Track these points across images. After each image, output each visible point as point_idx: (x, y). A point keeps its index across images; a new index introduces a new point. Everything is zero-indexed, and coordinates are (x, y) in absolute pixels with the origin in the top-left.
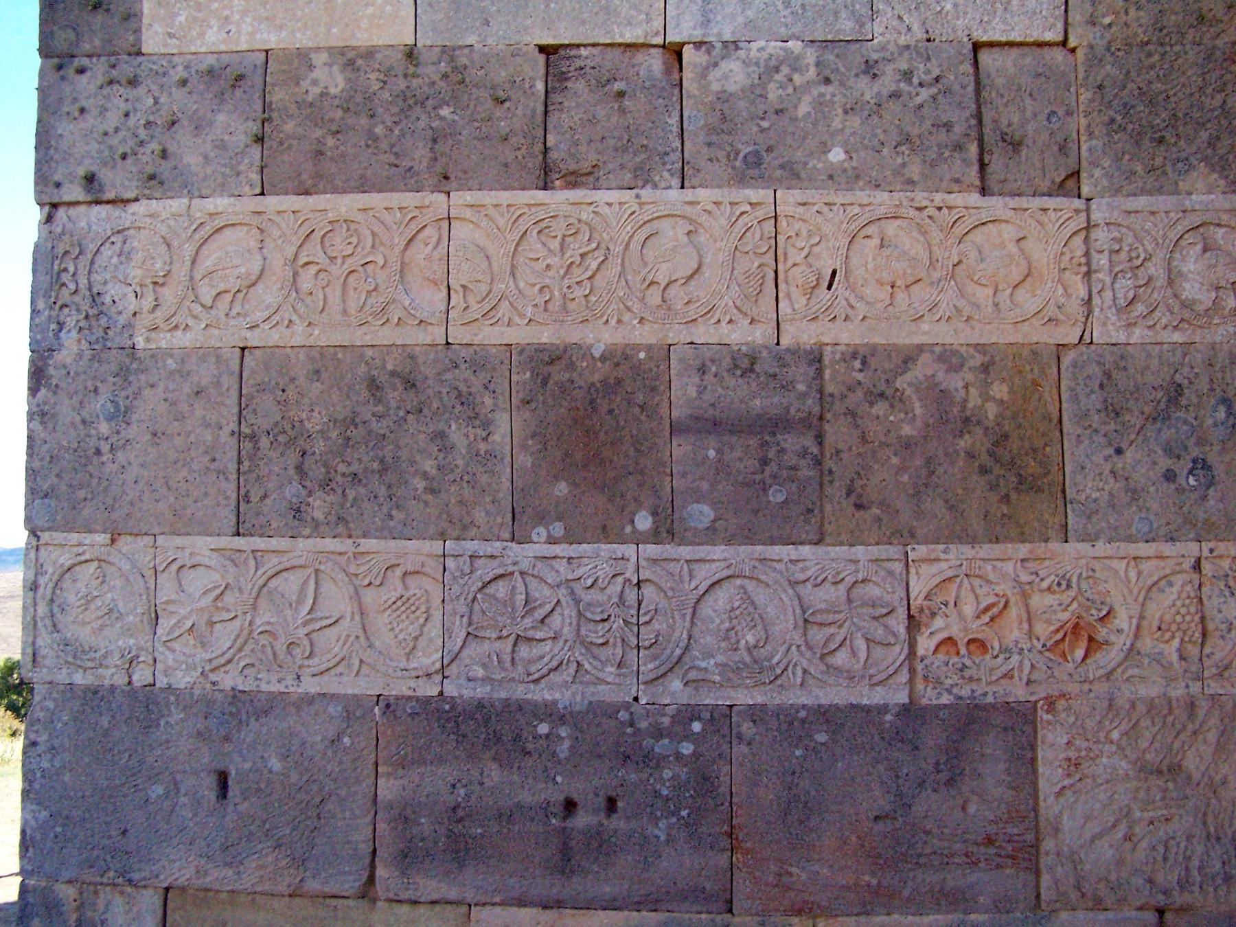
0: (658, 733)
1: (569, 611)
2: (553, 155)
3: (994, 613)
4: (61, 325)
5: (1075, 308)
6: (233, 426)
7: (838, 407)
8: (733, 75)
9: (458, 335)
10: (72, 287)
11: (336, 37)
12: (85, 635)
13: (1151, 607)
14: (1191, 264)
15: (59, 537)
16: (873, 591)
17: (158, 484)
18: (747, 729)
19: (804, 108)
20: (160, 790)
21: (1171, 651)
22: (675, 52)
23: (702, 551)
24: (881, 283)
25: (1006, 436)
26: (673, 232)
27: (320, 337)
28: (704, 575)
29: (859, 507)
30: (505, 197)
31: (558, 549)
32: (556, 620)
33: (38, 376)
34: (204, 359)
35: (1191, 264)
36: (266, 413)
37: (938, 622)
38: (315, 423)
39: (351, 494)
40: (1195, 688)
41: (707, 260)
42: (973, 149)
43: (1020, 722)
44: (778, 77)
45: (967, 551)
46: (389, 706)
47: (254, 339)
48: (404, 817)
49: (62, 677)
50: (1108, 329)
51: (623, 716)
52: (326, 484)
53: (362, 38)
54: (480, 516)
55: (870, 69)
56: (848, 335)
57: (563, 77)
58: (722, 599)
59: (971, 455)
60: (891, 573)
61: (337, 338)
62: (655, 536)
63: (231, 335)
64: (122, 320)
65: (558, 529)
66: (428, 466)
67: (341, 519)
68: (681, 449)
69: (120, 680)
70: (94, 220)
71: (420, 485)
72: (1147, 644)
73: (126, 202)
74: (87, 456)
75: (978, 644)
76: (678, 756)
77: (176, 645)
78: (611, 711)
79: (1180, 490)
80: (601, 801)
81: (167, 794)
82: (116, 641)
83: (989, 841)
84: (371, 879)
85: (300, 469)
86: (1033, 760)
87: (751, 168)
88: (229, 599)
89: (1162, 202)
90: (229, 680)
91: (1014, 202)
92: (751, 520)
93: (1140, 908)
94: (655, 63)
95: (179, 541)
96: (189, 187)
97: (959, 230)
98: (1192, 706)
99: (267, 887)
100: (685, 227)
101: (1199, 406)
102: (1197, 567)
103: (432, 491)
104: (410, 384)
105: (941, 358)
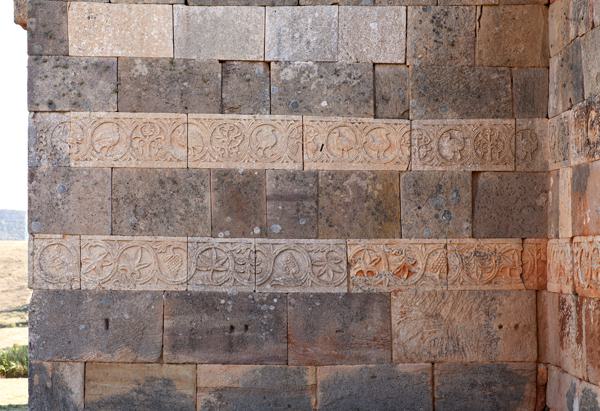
0: (262, 303)
1: (231, 261)
2: (225, 101)
3: (376, 262)
4: (41, 157)
5: (405, 158)
6: (109, 196)
7: (323, 192)
8: (288, 74)
9: (192, 165)
10: (44, 143)
11: (144, 53)
12: (53, 271)
13: (430, 260)
14: (446, 143)
15: (43, 236)
16: (335, 254)
17: (82, 216)
18: (293, 301)
19: (313, 86)
20: (83, 327)
21: (437, 276)
22: (269, 63)
23: (277, 241)
24: (339, 149)
25: (381, 202)
26: (267, 130)
27: (142, 165)
28: (278, 249)
29: (330, 226)
30: (208, 116)
31: (227, 240)
32: (227, 265)
33: (32, 176)
34: (98, 171)
35: (446, 143)
36: (122, 191)
37: (357, 265)
38: (140, 195)
39: (154, 221)
40: (445, 288)
41: (279, 139)
42: (372, 102)
43: (385, 299)
44: (305, 75)
45: (367, 241)
46: (168, 294)
47: (116, 165)
48: (173, 334)
49: (44, 287)
50: (417, 166)
51: (250, 296)
52: (145, 216)
53: (153, 55)
54: (200, 229)
55: (337, 73)
56: (327, 167)
57: (228, 72)
58: (283, 258)
59: (369, 209)
60: (341, 248)
61: (148, 165)
62: (261, 236)
63: (109, 163)
64: (64, 156)
65: (227, 233)
66: (182, 211)
67: (150, 230)
68: (270, 206)
69: (68, 288)
70: (52, 118)
71: (179, 217)
72: (428, 273)
73: (64, 112)
74: (53, 206)
75: (371, 273)
76: (269, 310)
77: (89, 275)
78: (245, 295)
79: (440, 222)
80: (243, 327)
81: (86, 328)
82: (64, 273)
83: (375, 339)
84: (162, 356)
85: (134, 211)
86: (390, 312)
87: (294, 108)
88: (109, 258)
89: (437, 122)
90: (109, 286)
91: (385, 121)
92: (293, 230)
93: (426, 362)
94: (260, 68)
95: (90, 237)
96: (88, 107)
97: (366, 131)
98: (443, 294)
99: (123, 360)
100: (271, 128)
101: (447, 192)
102: (446, 247)
103: (182, 219)
104: (175, 182)
105: (359, 175)
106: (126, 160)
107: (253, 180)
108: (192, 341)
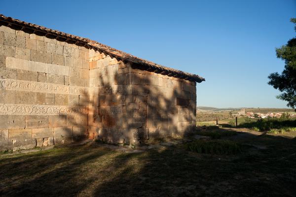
8: (50, 76)
53: (25, 69)
68: (46, 99)
94: (45, 74)
96: (11, 78)
106: (19, 89)
107: (43, 95)
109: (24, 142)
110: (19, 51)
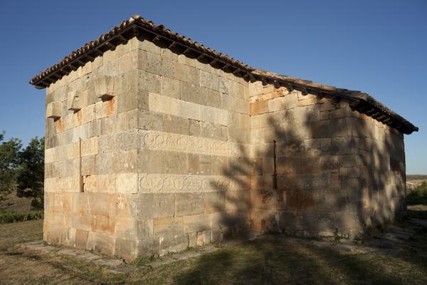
8: (205, 126)
53: (173, 114)
104: (178, 156)
106: (167, 147)
108: (182, 209)
109: (174, 240)
110: (165, 83)
